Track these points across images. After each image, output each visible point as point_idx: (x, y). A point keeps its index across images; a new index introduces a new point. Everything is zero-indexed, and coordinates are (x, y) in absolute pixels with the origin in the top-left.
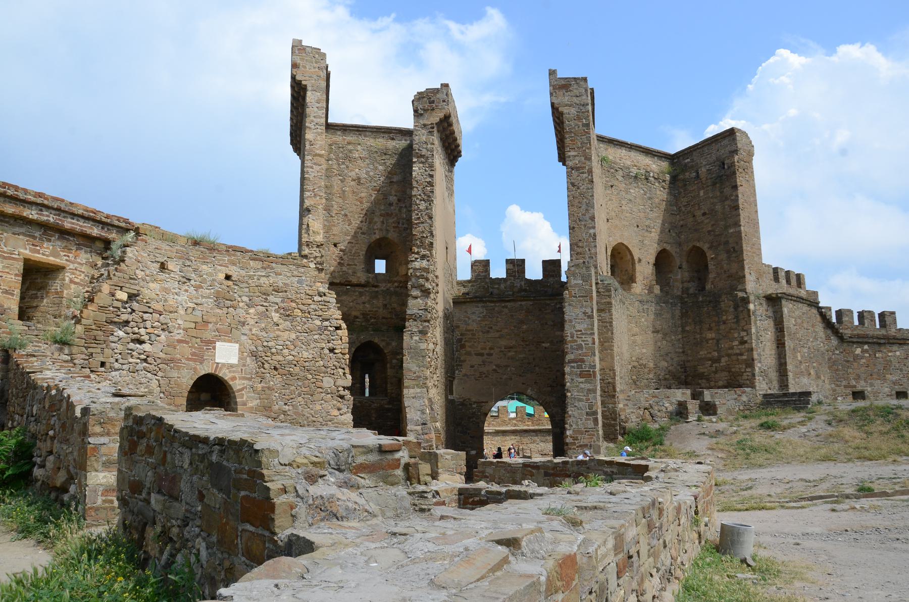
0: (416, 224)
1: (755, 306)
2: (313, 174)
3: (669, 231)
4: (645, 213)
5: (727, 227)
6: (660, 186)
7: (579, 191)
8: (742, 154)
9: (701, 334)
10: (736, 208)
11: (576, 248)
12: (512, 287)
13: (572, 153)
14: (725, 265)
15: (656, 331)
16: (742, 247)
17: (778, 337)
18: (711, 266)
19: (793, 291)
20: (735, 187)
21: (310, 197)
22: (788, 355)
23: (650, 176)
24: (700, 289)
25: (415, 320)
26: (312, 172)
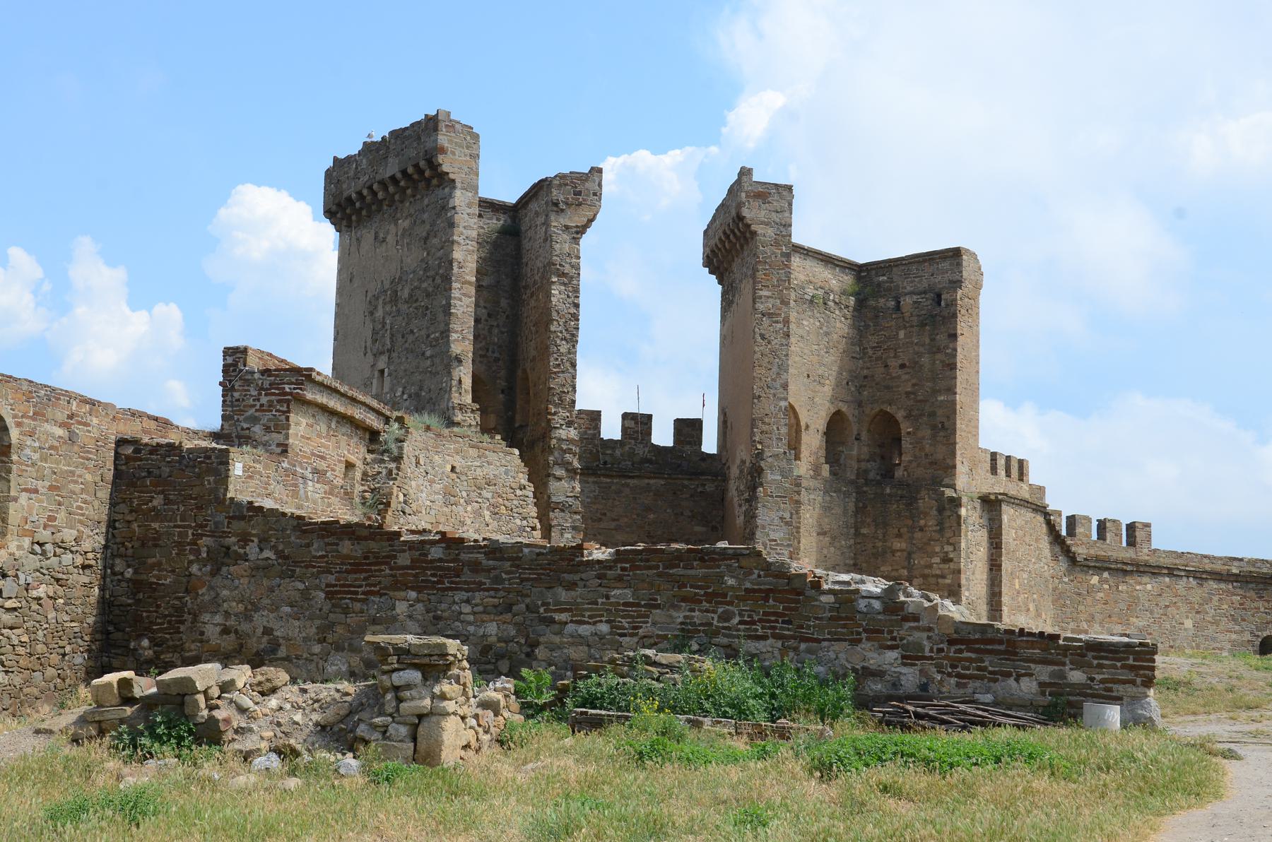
0: (555, 373)
1: (967, 510)
2: (462, 309)
3: (848, 383)
4: (818, 355)
5: (935, 392)
6: (841, 315)
7: (769, 346)
8: (967, 286)
9: (885, 541)
10: (953, 367)
11: (760, 424)
12: (632, 454)
13: (765, 293)
14: (927, 446)
15: (822, 533)
16: (955, 424)
17: (992, 554)
18: (906, 444)
19: (1012, 488)
20: (953, 336)
21: (458, 341)
22: (1004, 581)
23: (829, 300)
24: (883, 472)
25: (563, 511)
26: (461, 306)
